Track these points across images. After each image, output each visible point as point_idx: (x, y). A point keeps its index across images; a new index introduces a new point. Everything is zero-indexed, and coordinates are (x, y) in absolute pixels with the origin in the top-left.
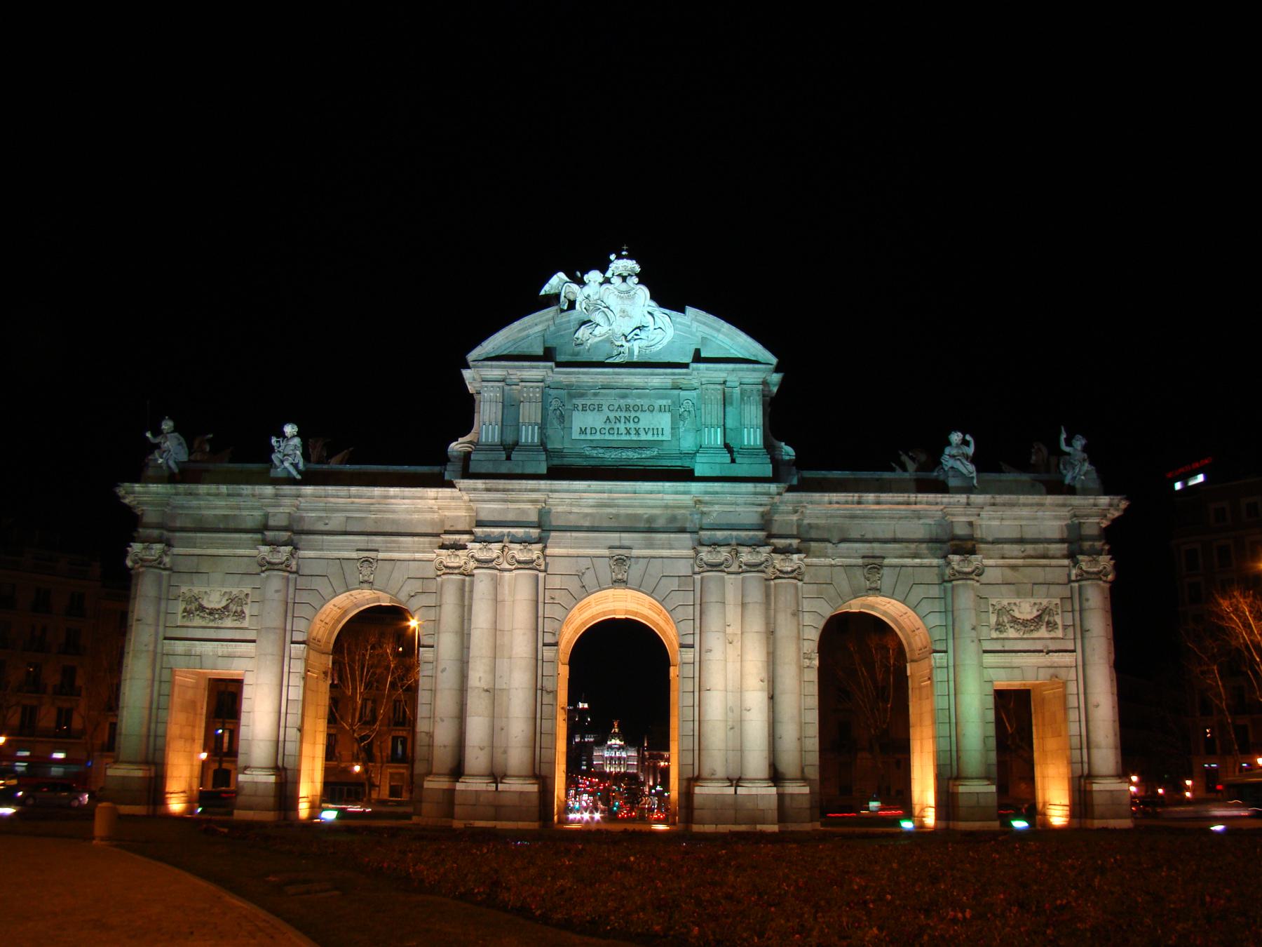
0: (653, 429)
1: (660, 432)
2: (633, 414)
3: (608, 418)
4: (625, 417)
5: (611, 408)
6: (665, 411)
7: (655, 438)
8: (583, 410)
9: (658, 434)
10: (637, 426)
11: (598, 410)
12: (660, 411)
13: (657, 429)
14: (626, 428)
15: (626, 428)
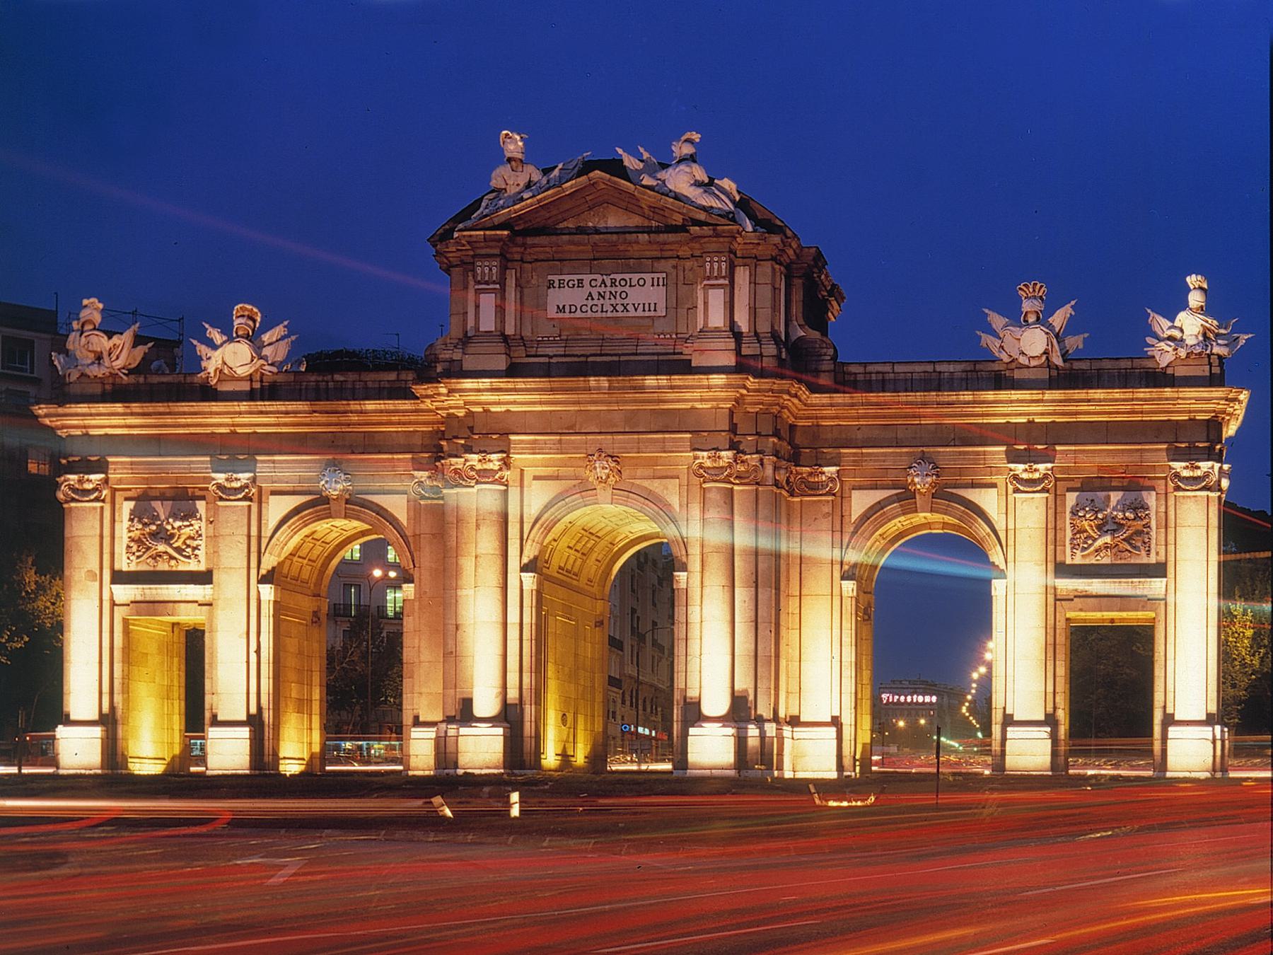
0: (644, 304)
1: (652, 309)
2: (619, 289)
3: (590, 293)
4: (611, 293)
5: (593, 285)
6: (658, 285)
7: (647, 314)
8: (559, 287)
9: (650, 310)
10: (625, 302)
11: (578, 287)
12: (653, 285)
13: (649, 304)
14: (612, 305)
15: (612, 305)
